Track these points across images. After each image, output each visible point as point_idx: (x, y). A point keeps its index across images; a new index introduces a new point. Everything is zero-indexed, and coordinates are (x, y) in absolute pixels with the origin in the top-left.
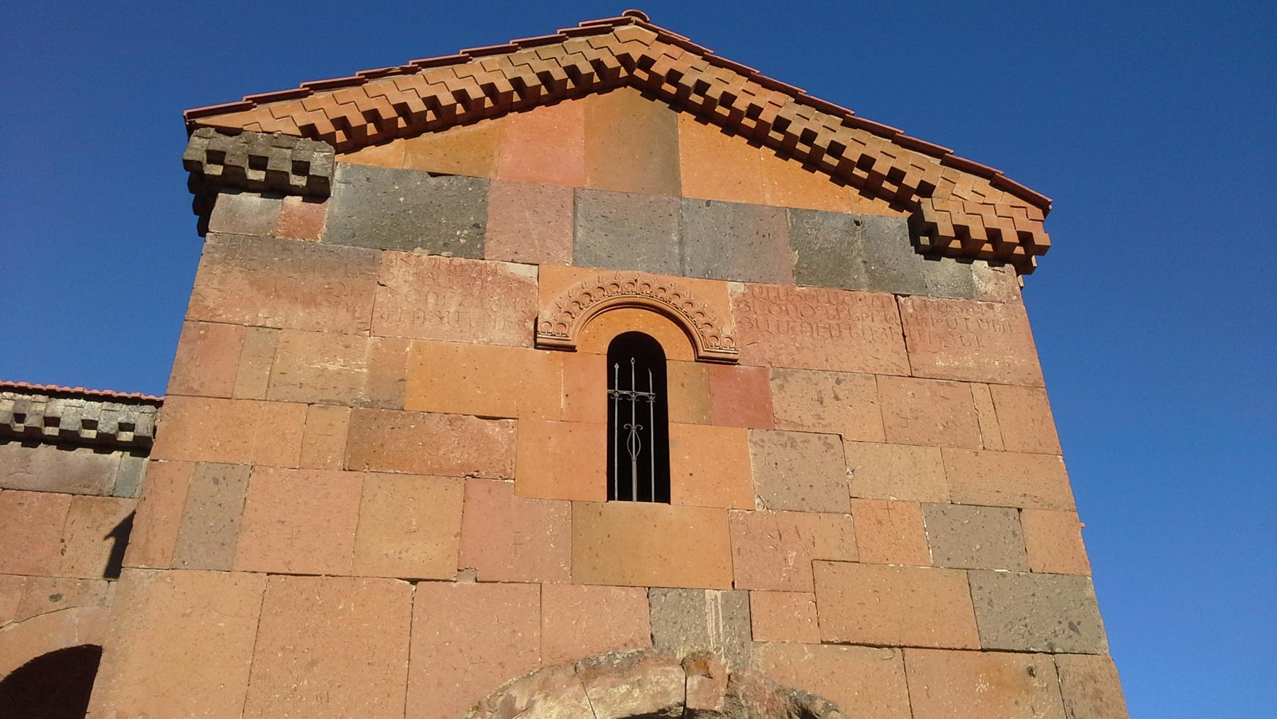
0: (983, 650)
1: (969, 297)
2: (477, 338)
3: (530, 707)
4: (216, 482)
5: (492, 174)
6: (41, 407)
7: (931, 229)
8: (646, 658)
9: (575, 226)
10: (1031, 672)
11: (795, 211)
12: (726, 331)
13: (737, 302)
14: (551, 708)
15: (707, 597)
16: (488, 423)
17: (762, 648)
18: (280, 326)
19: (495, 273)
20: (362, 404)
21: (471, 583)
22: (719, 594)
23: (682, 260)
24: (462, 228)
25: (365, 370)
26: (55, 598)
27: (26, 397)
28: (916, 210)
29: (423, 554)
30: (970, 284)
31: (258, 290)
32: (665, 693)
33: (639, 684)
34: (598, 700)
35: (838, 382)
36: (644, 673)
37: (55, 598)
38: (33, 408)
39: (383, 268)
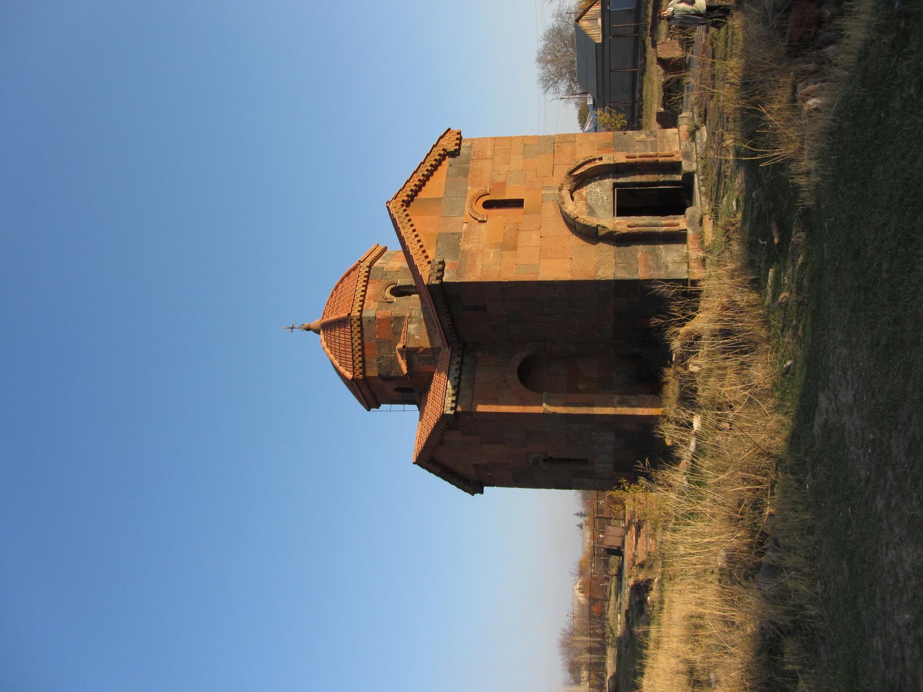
7: (456, 150)
29: (535, 236)
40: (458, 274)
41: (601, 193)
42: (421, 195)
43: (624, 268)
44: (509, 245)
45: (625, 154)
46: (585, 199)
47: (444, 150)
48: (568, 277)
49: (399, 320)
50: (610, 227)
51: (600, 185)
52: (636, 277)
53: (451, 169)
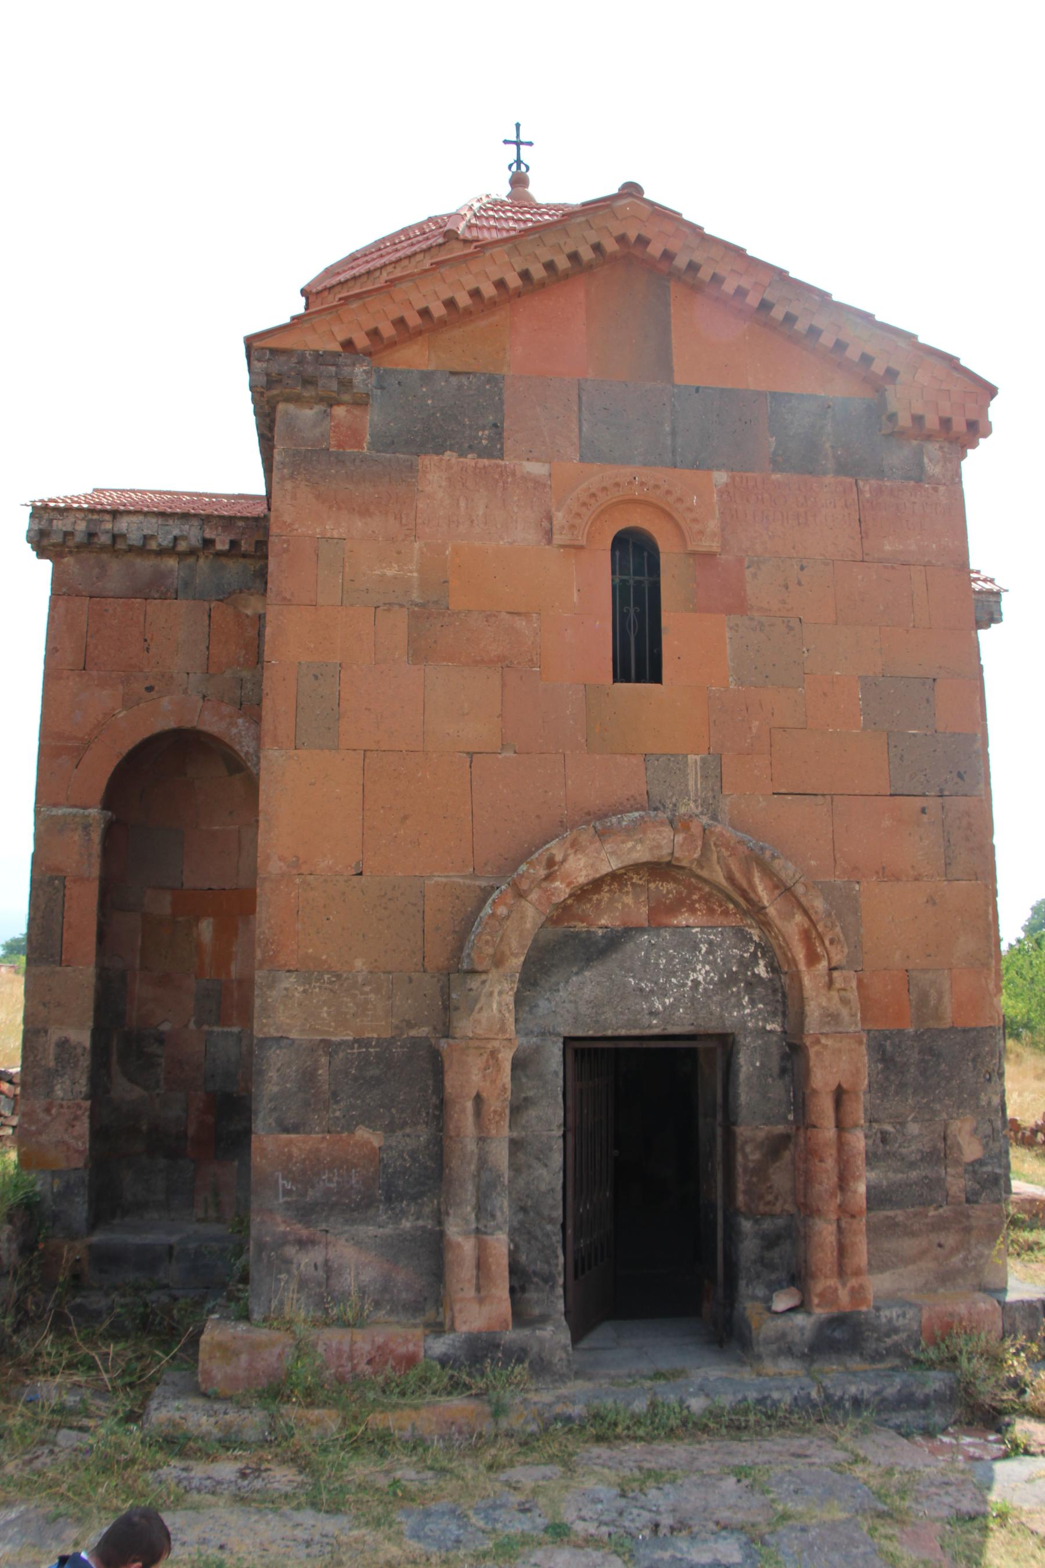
0: (891, 795)
1: (919, 481)
2: (503, 539)
3: (564, 860)
4: (316, 677)
6: (108, 526)
7: (892, 417)
8: (645, 822)
9: (580, 421)
10: (923, 811)
13: (721, 492)
14: (579, 859)
15: (689, 760)
16: (517, 618)
17: (729, 799)
18: (344, 536)
19: (514, 474)
20: (416, 605)
21: (511, 754)
22: (698, 757)
23: (674, 452)
24: (483, 428)
25: (415, 574)
26: (150, 689)
27: (95, 517)
28: (880, 391)
30: (921, 466)
31: (323, 503)
32: (659, 847)
33: (641, 841)
34: (613, 853)
35: (802, 568)
36: (645, 833)
37: (150, 689)
38: (103, 527)
39: (420, 474)
43: (308, 1077)
46: (655, 924)
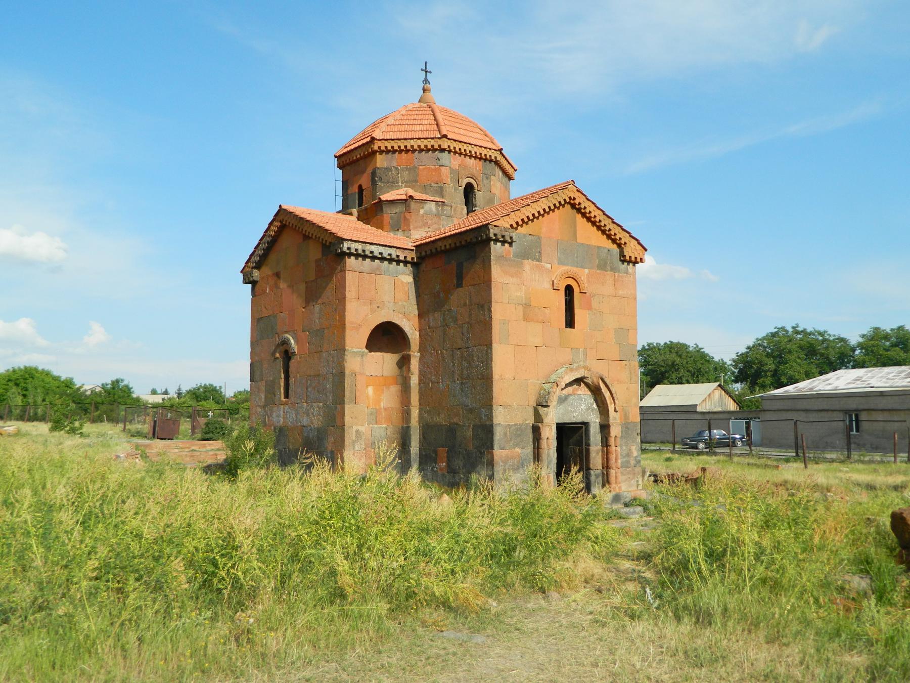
5: (542, 236)
7: (624, 256)
11: (598, 247)
12: (586, 286)
29: (538, 341)
40: (501, 257)
41: (581, 408)
42: (580, 221)
43: (505, 434)
44: (528, 311)
45: (619, 435)
46: (574, 394)
47: (625, 243)
48: (496, 376)
49: (441, 192)
50: (546, 420)
51: (588, 409)
52: (496, 447)
53: (606, 251)
